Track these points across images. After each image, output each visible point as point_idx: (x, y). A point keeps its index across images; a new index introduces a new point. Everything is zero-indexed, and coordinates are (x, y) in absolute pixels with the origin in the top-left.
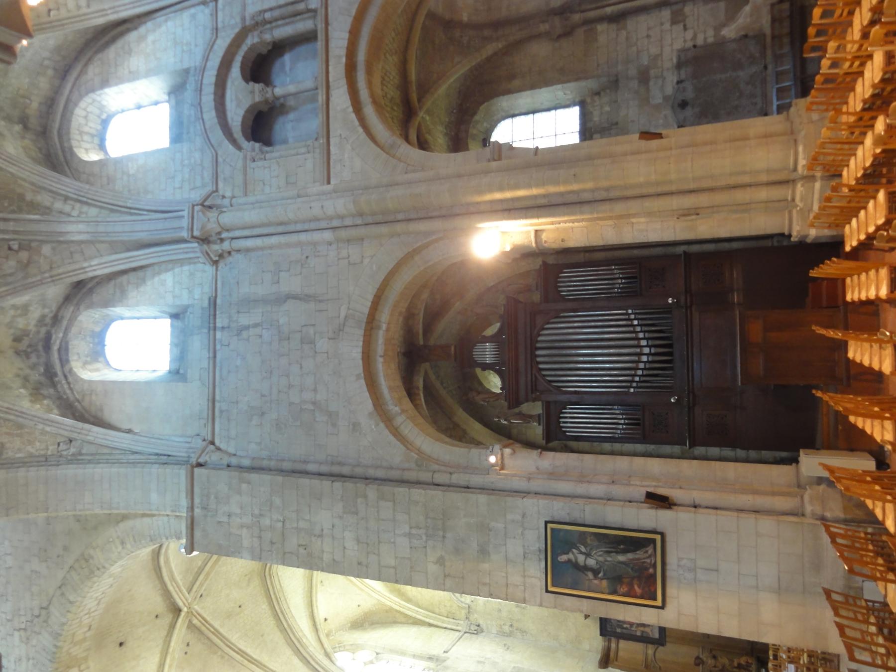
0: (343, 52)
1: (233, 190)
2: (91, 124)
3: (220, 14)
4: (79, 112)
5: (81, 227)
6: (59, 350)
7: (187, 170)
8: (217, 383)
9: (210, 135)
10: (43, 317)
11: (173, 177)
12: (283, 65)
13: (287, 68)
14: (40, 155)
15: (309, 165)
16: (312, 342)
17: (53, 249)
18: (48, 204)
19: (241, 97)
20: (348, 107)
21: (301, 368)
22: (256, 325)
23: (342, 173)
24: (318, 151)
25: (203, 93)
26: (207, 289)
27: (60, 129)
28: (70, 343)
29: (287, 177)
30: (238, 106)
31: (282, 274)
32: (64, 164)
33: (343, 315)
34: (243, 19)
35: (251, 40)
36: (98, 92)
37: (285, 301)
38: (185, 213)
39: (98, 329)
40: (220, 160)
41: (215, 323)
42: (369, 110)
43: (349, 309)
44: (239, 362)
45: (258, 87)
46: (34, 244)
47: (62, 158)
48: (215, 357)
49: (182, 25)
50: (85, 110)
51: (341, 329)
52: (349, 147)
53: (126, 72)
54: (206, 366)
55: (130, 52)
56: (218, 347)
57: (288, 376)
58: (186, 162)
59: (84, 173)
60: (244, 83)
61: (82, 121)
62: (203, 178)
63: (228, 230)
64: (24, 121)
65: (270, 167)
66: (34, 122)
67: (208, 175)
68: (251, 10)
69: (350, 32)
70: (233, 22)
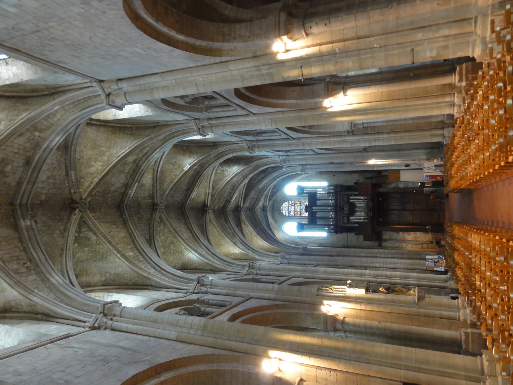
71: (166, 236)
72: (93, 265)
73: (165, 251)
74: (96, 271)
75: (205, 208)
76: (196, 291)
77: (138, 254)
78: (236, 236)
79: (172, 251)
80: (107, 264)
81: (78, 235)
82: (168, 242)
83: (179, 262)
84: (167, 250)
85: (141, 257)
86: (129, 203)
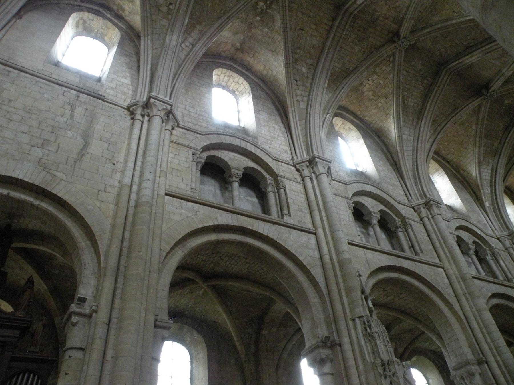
0: (255, 228)
1: (176, 136)
2: (233, 84)
3: (286, 165)
4: (241, 80)
5: (174, 43)
6: (99, 11)
7: (196, 116)
8: (35, 78)
9: (215, 135)
10: (124, 10)
11: (193, 107)
12: (251, 196)
13: (249, 198)
14: (221, 50)
15: (183, 186)
16: (42, 146)
17: (164, 26)
18: (193, 34)
19: (237, 162)
20: (218, 221)
21: (23, 132)
22: (72, 116)
23: (171, 204)
24: (192, 194)
25: (242, 141)
26: (111, 97)
27: (234, 67)
28: (102, 18)
29: (178, 170)
30: (231, 159)
31: (106, 145)
32: (213, 60)
33: (58, 174)
34: (282, 177)
35: (270, 179)
36: (250, 92)
37: (84, 140)
38: (168, 99)
39: (106, 38)
40: (198, 136)
41: (84, 93)
42: (213, 237)
43: (61, 179)
44: (46, 96)
45: (241, 173)
46: (170, 16)
47: (217, 60)
48: (57, 84)
49: (281, 144)
50: (242, 83)
51: (45, 168)
52: (190, 215)
53: (260, 109)
54: (53, 76)
55: (270, 114)
56: (64, 89)
57: (20, 122)
58: (201, 117)
59: (206, 67)
60: (244, 166)
61: (236, 80)
62: (189, 122)
63: (149, 121)
64: (241, 50)
65: (186, 161)
66: (239, 55)
67: (190, 125)
68: (287, 183)
69: (267, 236)
70: (281, 170)
71: (385, 82)
72: (263, 52)
73: (372, 97)
74: (263, 59)
75: (483, 91)
76: (298, 166)
77: (310, 76)
78: (497, 157)
79: (380, 105)
80: (275, 61)
81: (267, 9)
82: (383, 91)
83: (378, 122)
84: (375, 98)
85: (310, 81)
86: (351, 9)
